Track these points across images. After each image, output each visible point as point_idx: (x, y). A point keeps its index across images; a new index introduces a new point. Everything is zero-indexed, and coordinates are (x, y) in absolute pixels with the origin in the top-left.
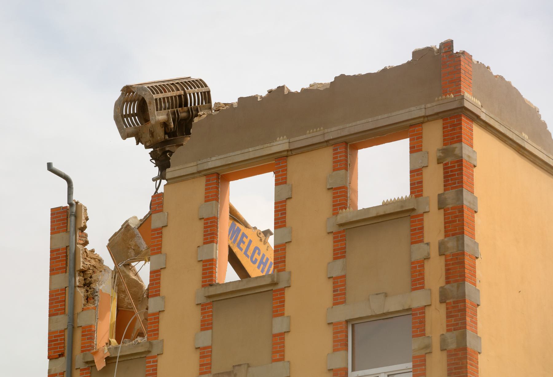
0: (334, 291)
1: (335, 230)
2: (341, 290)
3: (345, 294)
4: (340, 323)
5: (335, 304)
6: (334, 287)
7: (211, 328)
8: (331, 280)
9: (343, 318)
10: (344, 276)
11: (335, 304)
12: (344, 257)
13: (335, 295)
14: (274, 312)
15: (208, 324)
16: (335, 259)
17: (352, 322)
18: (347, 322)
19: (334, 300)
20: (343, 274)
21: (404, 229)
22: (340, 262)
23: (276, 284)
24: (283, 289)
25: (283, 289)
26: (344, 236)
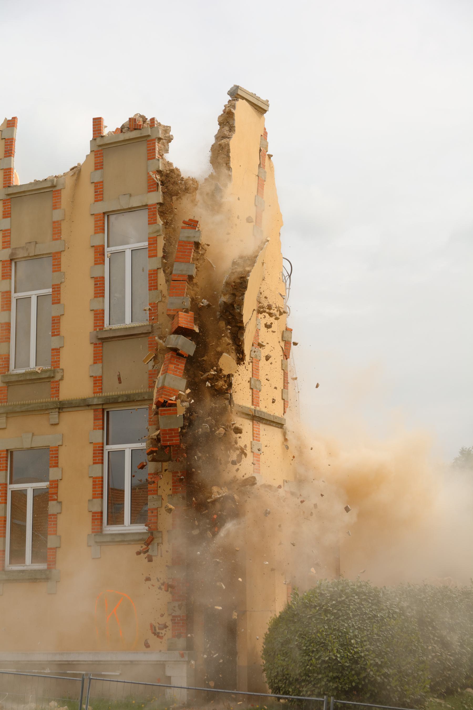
0: (95, 192)
1: (96, 149)
2: (100, 192)
3: (102, 194)
4: (99, 214)
5: (96, 201)
6: (95, 189)
7: (10, 217)
8: (93, 184)
9: (102, 211)
10: (102, 182)
11: (96, 201)
12: (102, 168)
13: (96, 195)
14: (53, 206)
15: (8, 214)
16: (96, 169)
17: (107, 214)
18: (104, 213)
19: (95, 198)
20: (101, 180)
21: (143, 149)
22: (99, 172)
23: (55, 186)
24: (60, 190)
25: (60, 190)
26: (102, 153)
